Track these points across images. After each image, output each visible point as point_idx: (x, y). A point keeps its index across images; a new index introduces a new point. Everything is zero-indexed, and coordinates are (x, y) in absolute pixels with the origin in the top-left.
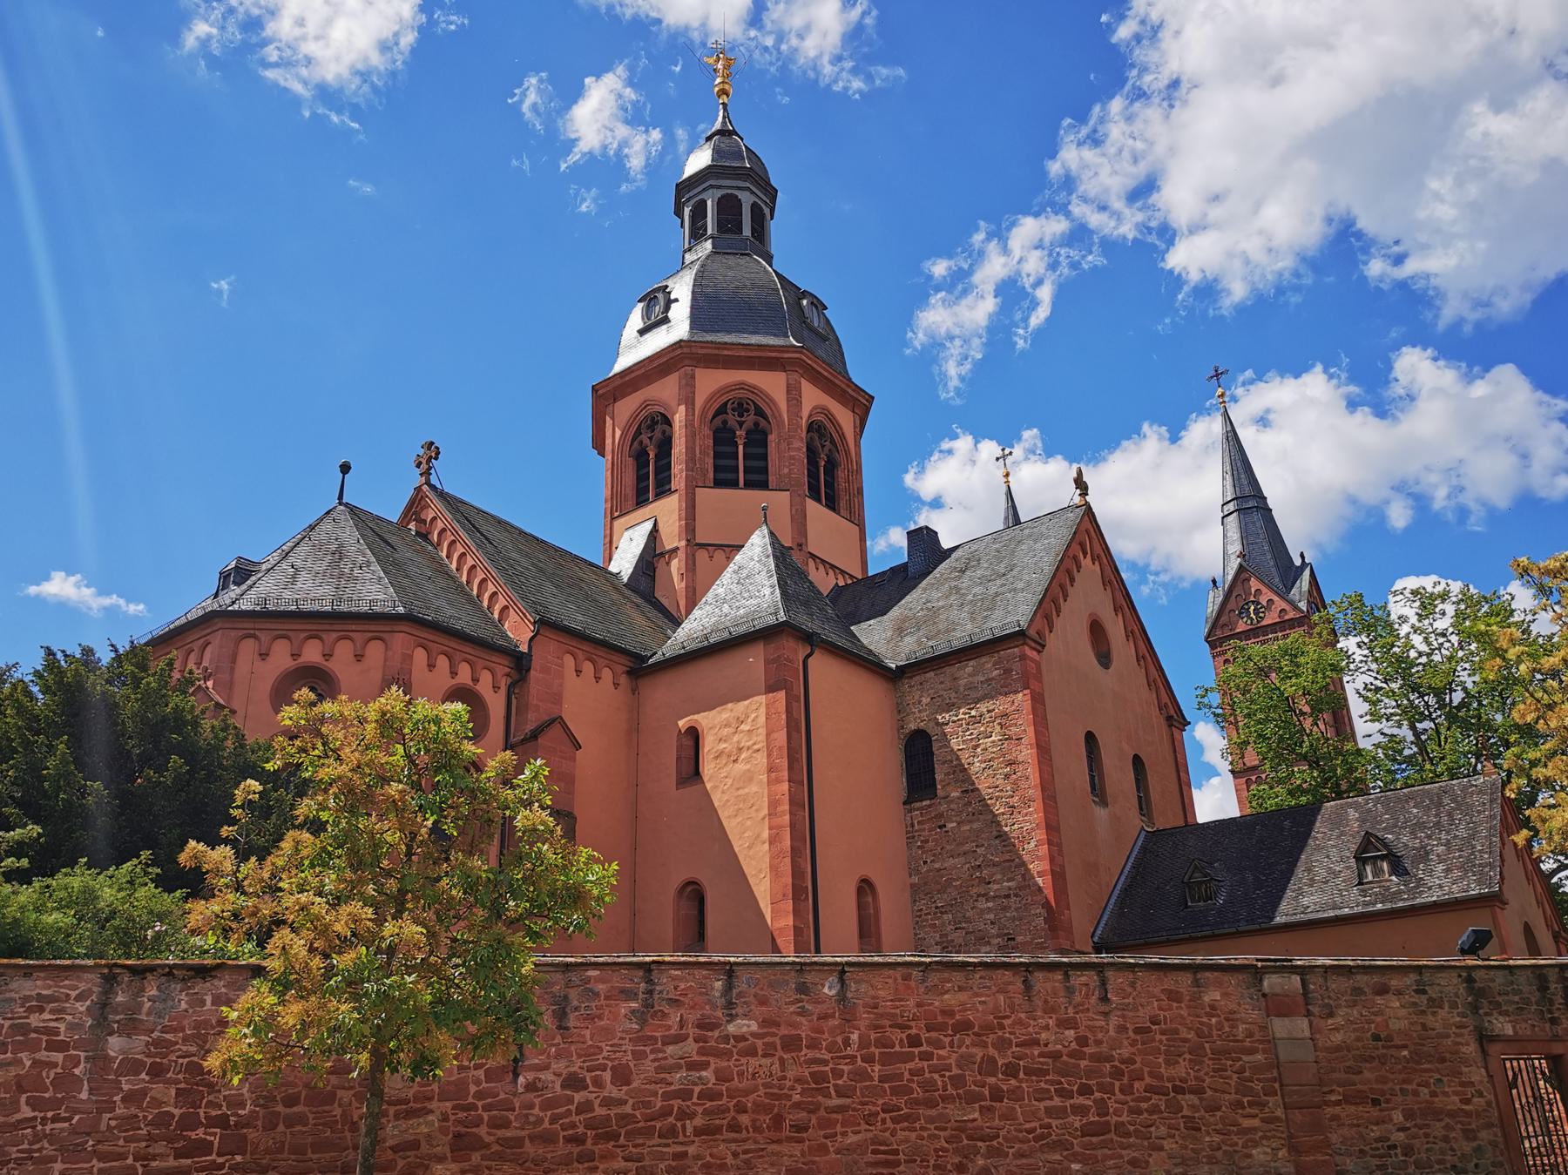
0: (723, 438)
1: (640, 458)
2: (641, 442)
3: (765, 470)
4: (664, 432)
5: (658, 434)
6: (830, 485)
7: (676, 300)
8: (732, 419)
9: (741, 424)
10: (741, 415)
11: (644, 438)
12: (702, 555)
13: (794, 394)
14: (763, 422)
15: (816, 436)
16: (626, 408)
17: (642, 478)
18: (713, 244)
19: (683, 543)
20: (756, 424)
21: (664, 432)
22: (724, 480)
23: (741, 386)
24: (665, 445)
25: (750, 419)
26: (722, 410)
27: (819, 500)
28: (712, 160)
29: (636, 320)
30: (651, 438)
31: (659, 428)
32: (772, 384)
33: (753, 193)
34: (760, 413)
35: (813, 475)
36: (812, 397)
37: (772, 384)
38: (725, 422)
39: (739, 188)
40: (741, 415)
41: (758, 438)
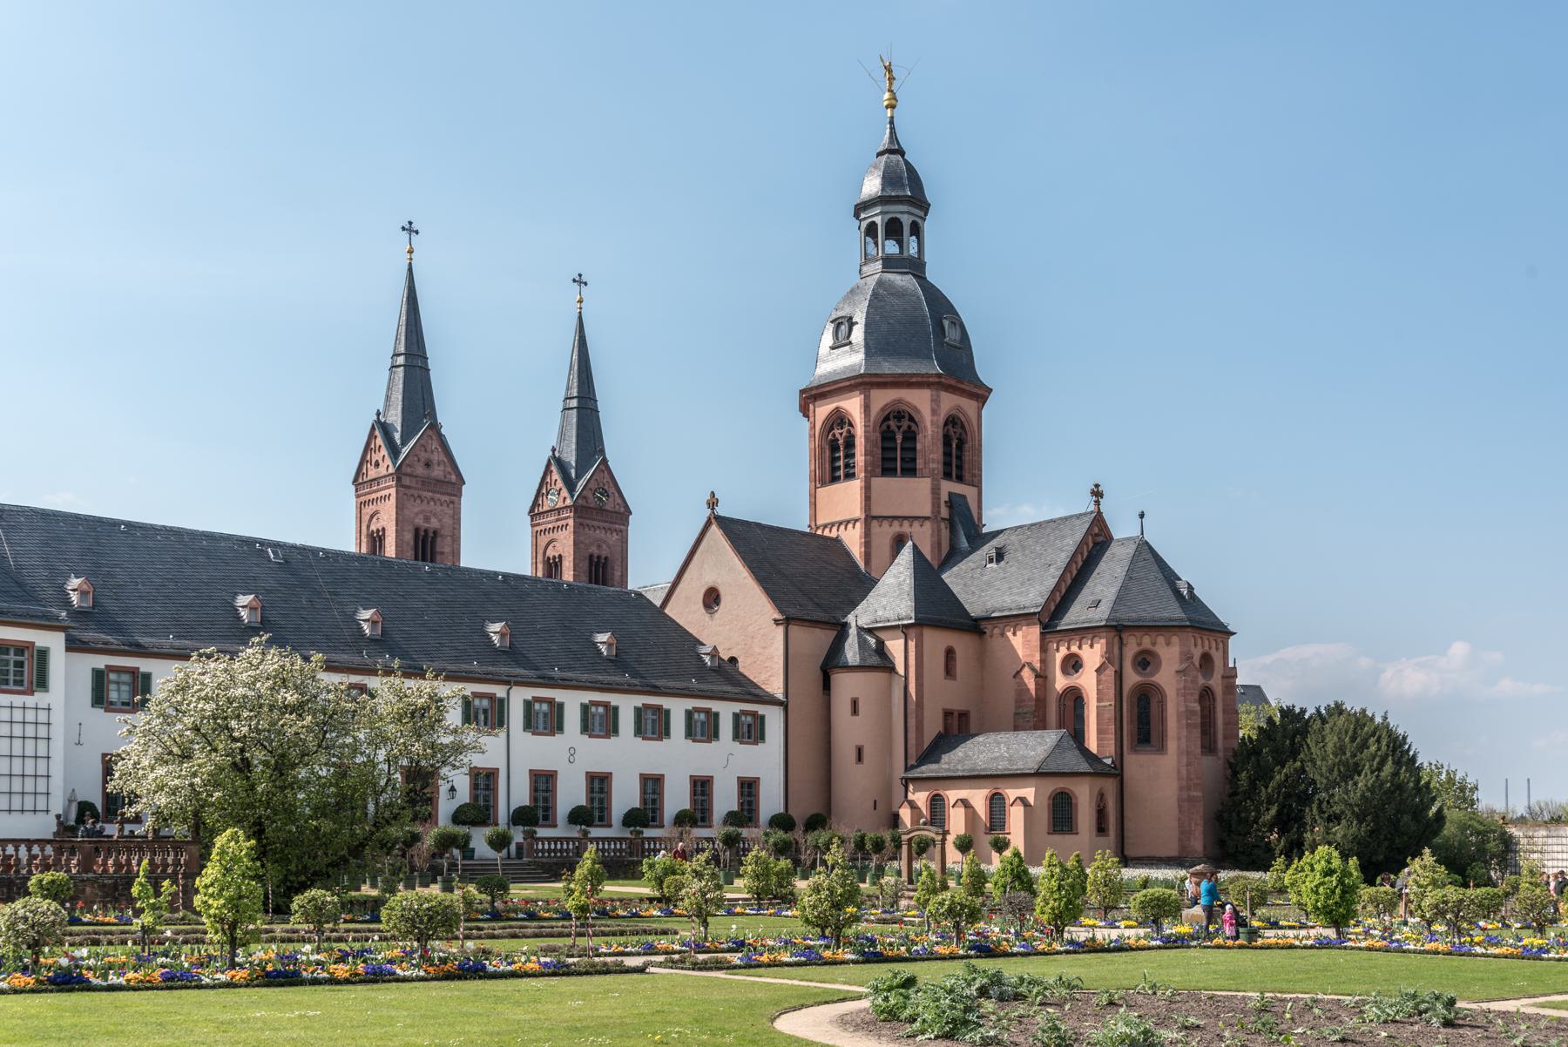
0: (887, 436)
1: (834, 448)
2: (834, 435)
3: (914, 460)
4: (849, 431)
5: (845, 430)
6: (959, 458)
7: (857, 323)
8: (892, 423)
9: (899, 427)
10: (899, 420)
11: (837, 432)
12: (875, 523)
13: (936, 401)
14: (914, 427)
15: (950, 427)
16: (823, 411)
17: (834, 459)
18: (883, 264)
19: (863, 517)
20: (909, 427)
21: (849, 431)
22: (888, 471)
23: (900, 401)
24: (850, 443)
25: (905, 423)
26: (887, 418)
27: (947, 475)
28: (883, 190)
29: (828, 339)
30: (841, 434)
31: (846, 428)
32: (920, 400)
33: (912, 214)
34: (911, 419)
35: (947, 454)
36: (949, 402)
37: (920, 400)
38: (889, 427)
39: (902, 213)
40: (899, 420)
41: (911, 437)
